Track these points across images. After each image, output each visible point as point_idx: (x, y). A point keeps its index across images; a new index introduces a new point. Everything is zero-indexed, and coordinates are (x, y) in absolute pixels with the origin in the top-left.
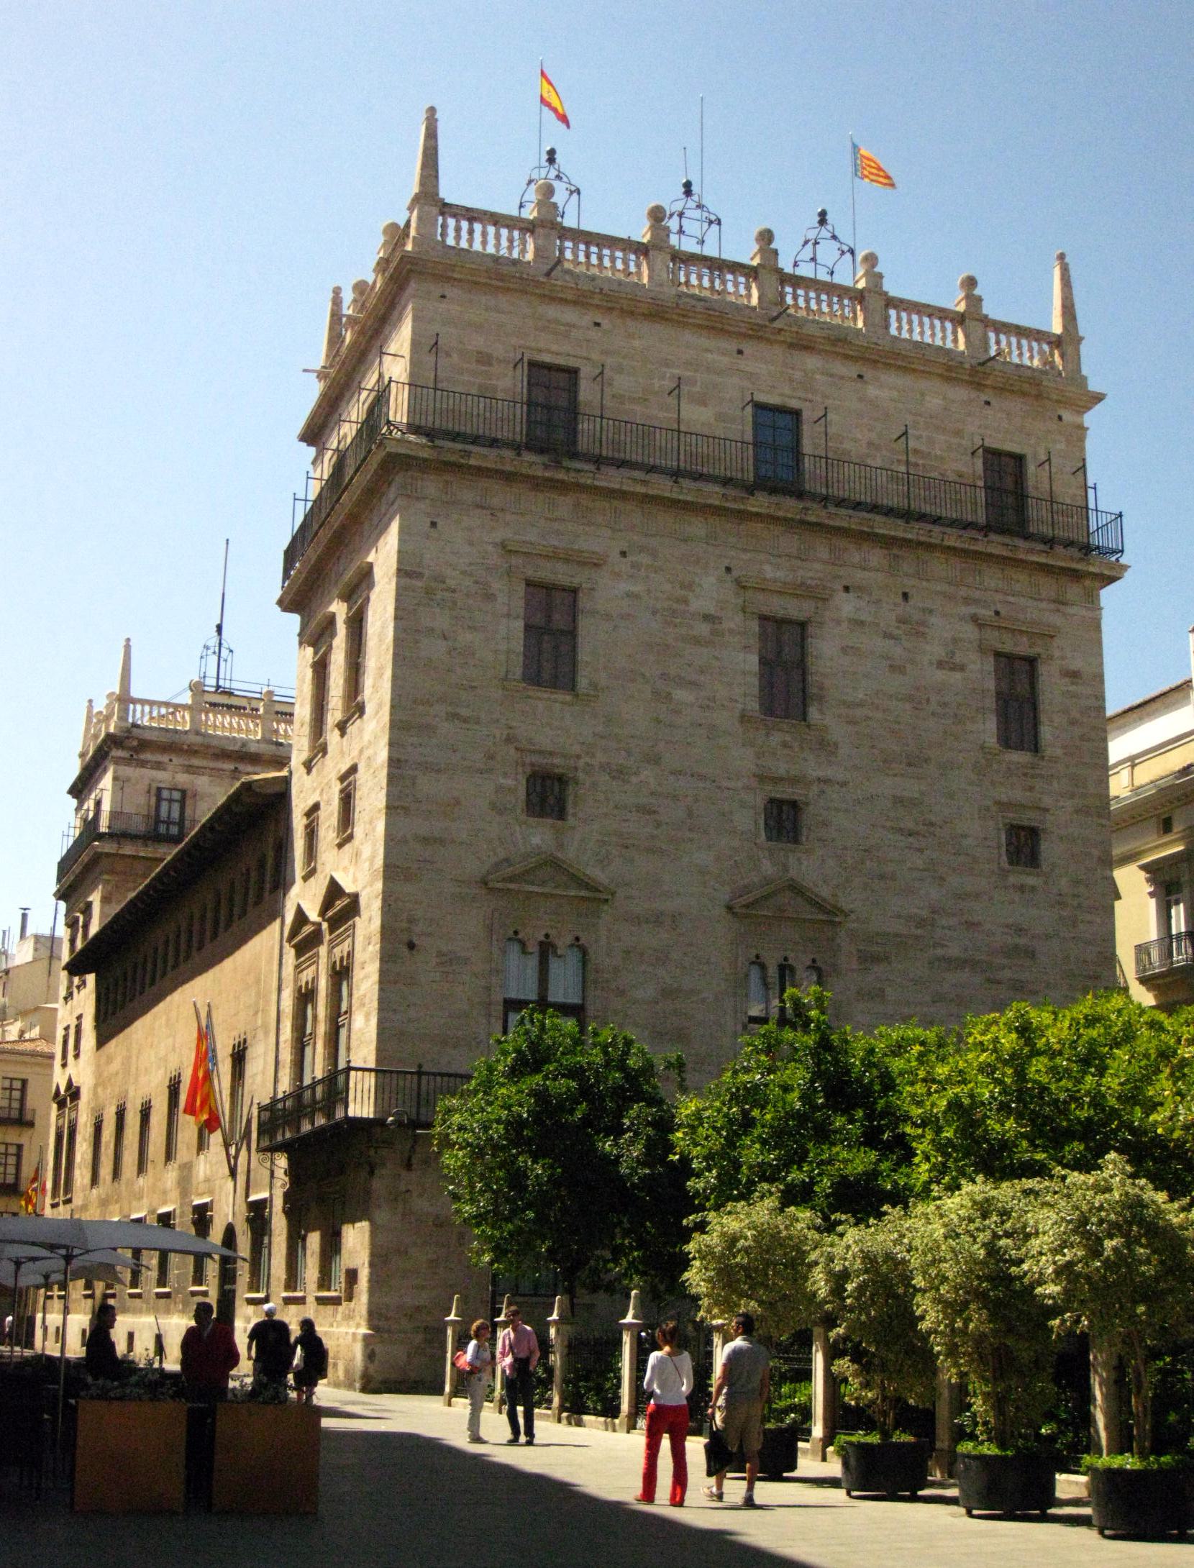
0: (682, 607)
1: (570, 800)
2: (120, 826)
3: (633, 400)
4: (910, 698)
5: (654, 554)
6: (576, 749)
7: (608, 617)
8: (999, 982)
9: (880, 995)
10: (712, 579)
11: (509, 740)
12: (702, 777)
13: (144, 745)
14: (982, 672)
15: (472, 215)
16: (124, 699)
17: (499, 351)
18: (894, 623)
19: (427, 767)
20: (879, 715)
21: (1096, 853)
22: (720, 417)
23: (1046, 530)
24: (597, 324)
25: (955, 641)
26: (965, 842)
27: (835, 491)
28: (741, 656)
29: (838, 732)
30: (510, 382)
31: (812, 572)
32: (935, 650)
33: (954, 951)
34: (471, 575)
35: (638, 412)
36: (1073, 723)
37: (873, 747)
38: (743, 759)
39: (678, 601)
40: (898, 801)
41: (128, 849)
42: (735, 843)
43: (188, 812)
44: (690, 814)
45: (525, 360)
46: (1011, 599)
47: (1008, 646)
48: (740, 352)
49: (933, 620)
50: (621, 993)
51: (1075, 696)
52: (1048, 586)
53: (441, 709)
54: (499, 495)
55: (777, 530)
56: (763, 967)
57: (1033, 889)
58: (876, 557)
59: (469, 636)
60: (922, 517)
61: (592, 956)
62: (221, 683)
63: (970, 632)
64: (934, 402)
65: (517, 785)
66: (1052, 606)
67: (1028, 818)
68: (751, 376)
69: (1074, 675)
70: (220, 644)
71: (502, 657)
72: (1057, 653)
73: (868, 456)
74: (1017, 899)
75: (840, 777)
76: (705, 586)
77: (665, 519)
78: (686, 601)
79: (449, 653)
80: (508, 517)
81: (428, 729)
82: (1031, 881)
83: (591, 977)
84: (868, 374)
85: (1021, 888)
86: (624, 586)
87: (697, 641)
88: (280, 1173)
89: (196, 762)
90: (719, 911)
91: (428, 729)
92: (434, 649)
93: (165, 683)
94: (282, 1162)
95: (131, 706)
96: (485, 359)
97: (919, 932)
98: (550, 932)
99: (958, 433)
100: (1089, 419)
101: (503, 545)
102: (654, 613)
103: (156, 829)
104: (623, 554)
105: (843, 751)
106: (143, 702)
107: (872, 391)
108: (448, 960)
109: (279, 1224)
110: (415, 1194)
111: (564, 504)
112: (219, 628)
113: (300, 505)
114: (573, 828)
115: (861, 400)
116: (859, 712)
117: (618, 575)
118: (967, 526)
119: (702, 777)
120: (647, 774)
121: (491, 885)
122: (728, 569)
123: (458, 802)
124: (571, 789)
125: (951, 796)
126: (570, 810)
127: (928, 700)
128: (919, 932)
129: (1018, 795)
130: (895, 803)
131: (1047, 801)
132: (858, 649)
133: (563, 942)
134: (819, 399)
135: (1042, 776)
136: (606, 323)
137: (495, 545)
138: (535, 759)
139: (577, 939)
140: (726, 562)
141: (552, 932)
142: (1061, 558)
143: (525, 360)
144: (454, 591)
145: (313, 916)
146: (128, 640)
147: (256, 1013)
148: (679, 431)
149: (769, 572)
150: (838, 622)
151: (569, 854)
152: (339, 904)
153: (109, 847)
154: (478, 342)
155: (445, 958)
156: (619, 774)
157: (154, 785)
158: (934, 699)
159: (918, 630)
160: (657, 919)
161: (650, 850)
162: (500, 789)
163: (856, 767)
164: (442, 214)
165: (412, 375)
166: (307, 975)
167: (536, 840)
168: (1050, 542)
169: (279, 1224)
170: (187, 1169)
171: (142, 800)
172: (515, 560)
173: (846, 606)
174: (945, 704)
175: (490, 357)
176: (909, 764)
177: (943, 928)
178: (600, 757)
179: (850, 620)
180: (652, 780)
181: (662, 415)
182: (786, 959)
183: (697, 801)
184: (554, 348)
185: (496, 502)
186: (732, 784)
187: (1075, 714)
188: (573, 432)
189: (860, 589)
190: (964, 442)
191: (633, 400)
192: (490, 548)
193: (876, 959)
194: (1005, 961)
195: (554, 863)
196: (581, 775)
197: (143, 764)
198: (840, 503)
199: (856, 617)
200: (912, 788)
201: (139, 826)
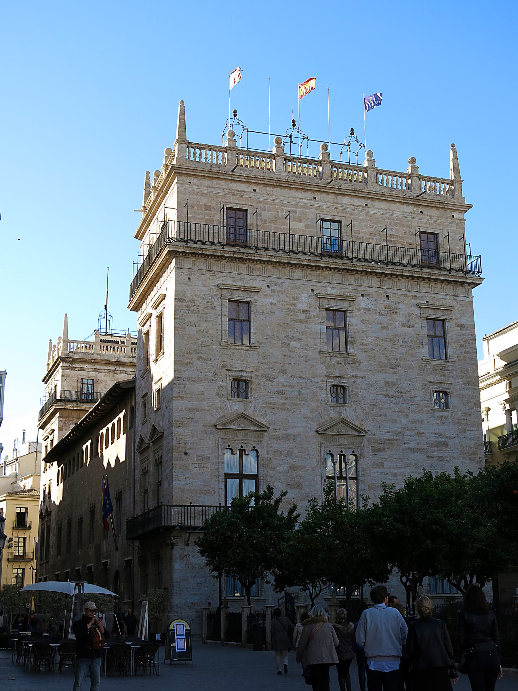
0: (294, 307)
2: (65, 396)
3: (271, 221)
4: (390, 340)
6: (251, 369)
8: (433, 458)
9: (382, 464)
10: (306, 295)
11: (223, 367)
12: (304, 378)
13: (75, 360)
14: (422, 327)
15: (201, 147)
17: (213, 204)
19: (189, 379)
20: (377, 348)
21: (474, 401)
22: (307, 226)
23: (448, 265)
25: (409, 315)
26: (416, 399)
27: (356, 255)
29: (360, 356)
30: (219, 218)
31: (347, 290)
33: (413, 445)
35: (272, 227)
36: (462, 346)
37: (375, 361)
38: (321, 370)
39: (291, 305)
40: (387, 383)
41: (69, 406)
42: (316, 407)
43: (95, 389)
45: (225, 207)
46: (433, 295)
47: (433, 315)
48: (315, 198)
49: (400, 306)
50: (273, 469)
51: (463, 335)
52: (450, 289)
53: (195, 355)
54: (215, 265)
55: (332, 273)
56: (332, 455)
58: (375, 281)
60: (394, 263)
61: (260, 454)
62: (108, 331)
63: (416, 310)
64: (398, 214)
65: (228, 384)
67: (442, 387)
68: (320, 208)
69: (462, 326)
70: (107, 314)
72: (453, 317)
73: (370, 238)
75: (362, 374)
77: (286, 271)
78: (295, 305)
81: (190, 364)
82: (445, 414)
83: (260, 463)
84: (369, 203)
86: (268, 300)
87: (300, 322)
88: (136, 548)
89: (98, 367)
90: (313, 433)
91: (190, 364)
92: (191, 330)
93: (83, 332)
94: (137, 544)
96: (208, 208)
97: (397, 438)
99: (409, 226)
100: (466, 216)
101: (218, 286)
102: (282, 310)
103: (81, 396)
104: (268, 286)
105: (363, 364)
106: (73, 342)
108: (202, 459)
109: (136, 569)
110: (191, 556)
111: (243, 267)
112: (106, 306)
113: (135, 266)
115: (366, 215)
117: (266, 296)
118: (414, 266)
119: (304, 378)
120: (281, 378)
122: (312, 290)
123: (203, 394)
125: (410, 380)
126: (249, 394)
128: (397, 438)
129: (438, 378)
130: (385, 384)
131: (451, 380)
134: (348, 215)
136: (257, 191)
137: (215, 286)
138: (235, 374)
139: (254, 447)
141: (244, 445)
142: (455, 276)
143: (225, 207)
144: (199, 306)
145: (146, 441)
147: (125, 480)
148: (290, 234)
149: (330, 291)
151: (250, 413)
152: (156, 436)
153: (60, 406)
154: (205, 201)
156: (269, 378)
157: (80, 378)
159: (393, 311)
160: (286, 438)
161: (283, 409)
163: (369, 370)
164: (188, 147)
165: (178, 217)
166: (145, 465)
167: (236, 407)
168: (450, 270)
169: (136, 569)
170: (98, 548)
171: (75, 384)
172: (223, 292)
173: (363, 303)
174: (406, 342)
175: (210, 207)
177: (408, 435)
178: (262, 372)
179: (365, 309)
180: (283, 380)
181: (282, 227)
182: (342, 452)
183: (302, 388)
184: (237, 202)
185: (215, 268)
187: (462, 343)
188: (245, 234)
189: (368, 295)
190: (411, 230)
191: (271, 221)
192: (213, 287)
193: (379, 450)
194: (435, 449)
195: (243, 416)
196: (254, 380)
197: (75, 369)
198: (359, 260)
200: (392, 378)
201: (73, 396)
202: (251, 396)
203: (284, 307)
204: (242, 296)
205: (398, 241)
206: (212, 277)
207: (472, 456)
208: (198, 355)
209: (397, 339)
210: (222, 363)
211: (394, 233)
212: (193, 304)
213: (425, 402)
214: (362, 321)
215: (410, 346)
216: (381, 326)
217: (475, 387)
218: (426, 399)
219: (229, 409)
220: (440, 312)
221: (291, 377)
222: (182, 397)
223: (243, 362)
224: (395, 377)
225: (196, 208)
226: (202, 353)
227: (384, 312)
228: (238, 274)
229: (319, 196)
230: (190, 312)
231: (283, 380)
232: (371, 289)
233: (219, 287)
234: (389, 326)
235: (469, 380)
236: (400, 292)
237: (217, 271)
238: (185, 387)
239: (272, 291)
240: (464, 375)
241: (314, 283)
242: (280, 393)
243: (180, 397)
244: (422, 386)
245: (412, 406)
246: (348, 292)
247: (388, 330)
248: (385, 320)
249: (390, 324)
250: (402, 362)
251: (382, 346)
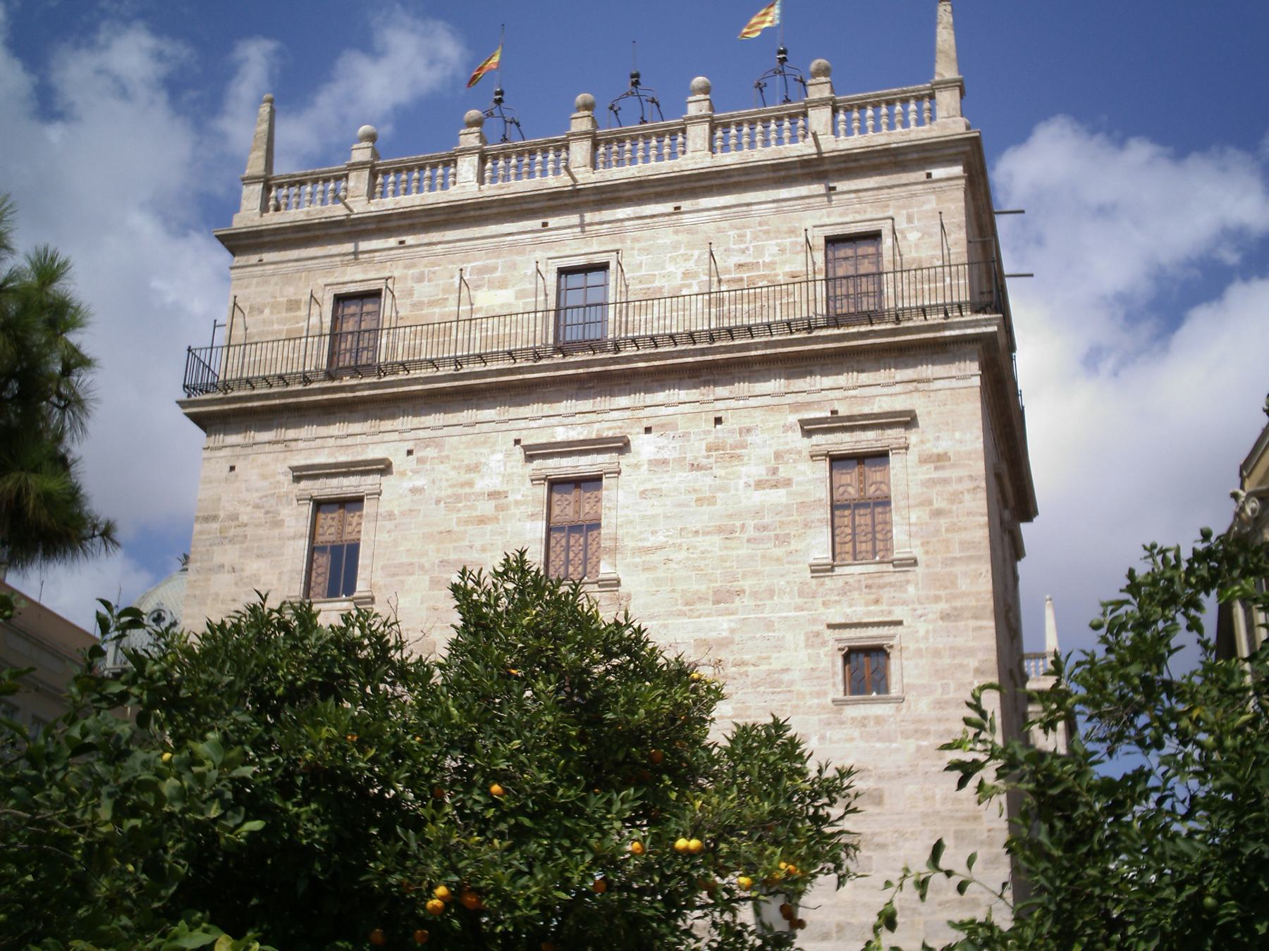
0: (467, 490)
3: (432, 304)
4: (720, 530)
5: (440, 446)
7: (391, 516)
10: (500, 456)
18: (705, 453)
22: (520, 295)
24: (402, 242)
26: (786, 677)
32: (755, 470)
36: (938, 513)
37: (673, 591)
39: (462, 485)
51: (945, 481)
57: (879, 720)
66: (911, 386)
69: (940, 460)
74: (856, 734)
76: (492, 464)
78: (470, 484)
79: (236, 584)
80: (301, 445)
85: (862, 722)
87: (482, 521)
116: (657, 557)
117: (403, 474)
127: (743, 526)
129: (858, 612)
132: (659, 490)
135: (891, 585)
140: (515, 435)
144: (246, 525)
149: (561, 435)
150: (637, 466)
158: (751, 523)
174: (765, 528)
176: (717, 602)
179: (650, 462)
189: (662, 426)
199: (659, 457)
203: (443, 494)
205: (759, 277)
206: (282, 456)
207: (966, 826)
209: (738, 524)
211: (750, 260)
212: (233, 524)
213: (815, 682)
214: (643, 492)
215: (777, 537)
216: (694, 496)
217: (980, 623)
218: (817, 674)
220: (871, 435)
224: (725, 626)
225: (267, 311)
227: (704, 461)
230: (226, 541)
232: (671, 410)
233: (300, 474)
234: (719, 495)
235: (958, 604)
236: (752, 402)
237: (296, 440)
239: (420, 461)
240: (942, 593)
244: (807, 639)
245: (773, 697)
246: (610, 429)
247: (714, 504)
248: (704, 481)
249: (723, 489)
250: (746, 584)
251: (695, 548)
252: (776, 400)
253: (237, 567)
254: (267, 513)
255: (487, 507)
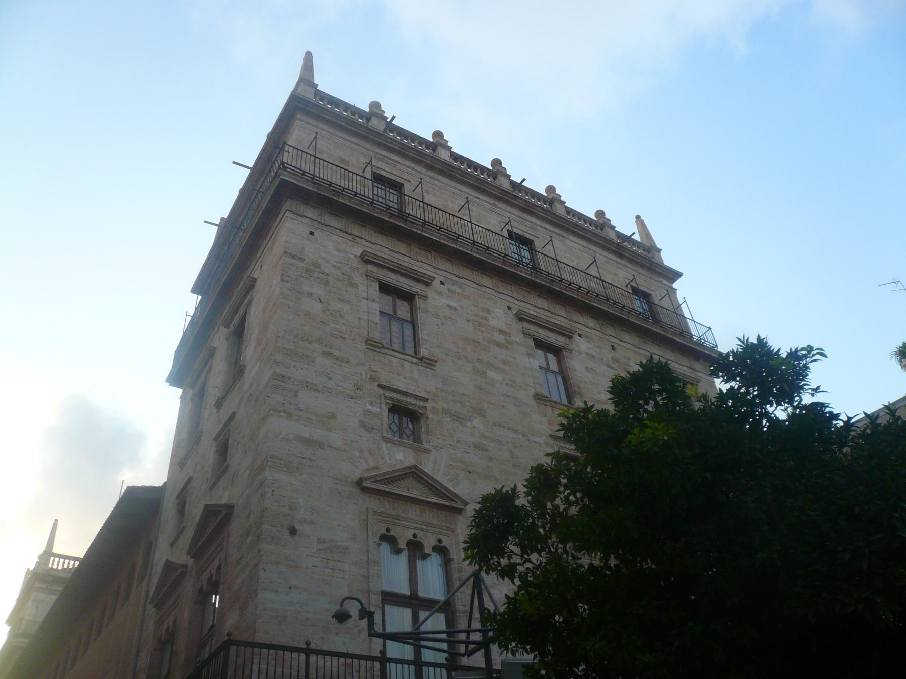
1: (423, 430)
7: (437, 316)
10: (501, 311)
11: (372, 379)
12: (516, 431)
16: (48, 553)
28: (527, 359)
34: (339, 268)
44: (511, 452)
59: (339, 305)
71: (364, 324)
79: (324, 311)
86: (444, 301)
87: (498, 344)
95: (52, 558)
98: (417, 532)
99: (616, 275)
100: (675, 285)
107: (567, 242)
111: (401, 247)
114: (427, 451)
117: (440, 293)
120: (477, 422)
121: (365, 484)
122: (509, 308)
123: (333, 417)
124: (423, 421)
126: (424, 437)
133: (429, 543)
137: (356, 256)
138: (394, 396)
141: (420, 534)
146: (56, 520)
151: (428, 469)
155: (326, 546)
162: (367, 413)
172: (371, 267)
180: (481, 427)
186: (536, 439)
192: (351, 256)
195: (415, 474)
196: (431, 416)
202: (428, 441)
204: (404, 283)
206: (351, 243)
208: (326, 349)
210: (370, 373)
212: (318, 269)
219: (387, 457)
221: (495, 424)
222: (289, 415)
223: (409, 379)
226: (332, 347)
228: (394, 251)
229: (499, 204)
231: (481, 427)
232: (589, 330)
236: (625, 344)
238: (296, 396)
239: (449, 290)
241: (511, 300)
242: (477, 446)
243: (285, 412)
252: (636, 349)
253: (323, 299)
254: (344, 274)
255: (501, 338)
